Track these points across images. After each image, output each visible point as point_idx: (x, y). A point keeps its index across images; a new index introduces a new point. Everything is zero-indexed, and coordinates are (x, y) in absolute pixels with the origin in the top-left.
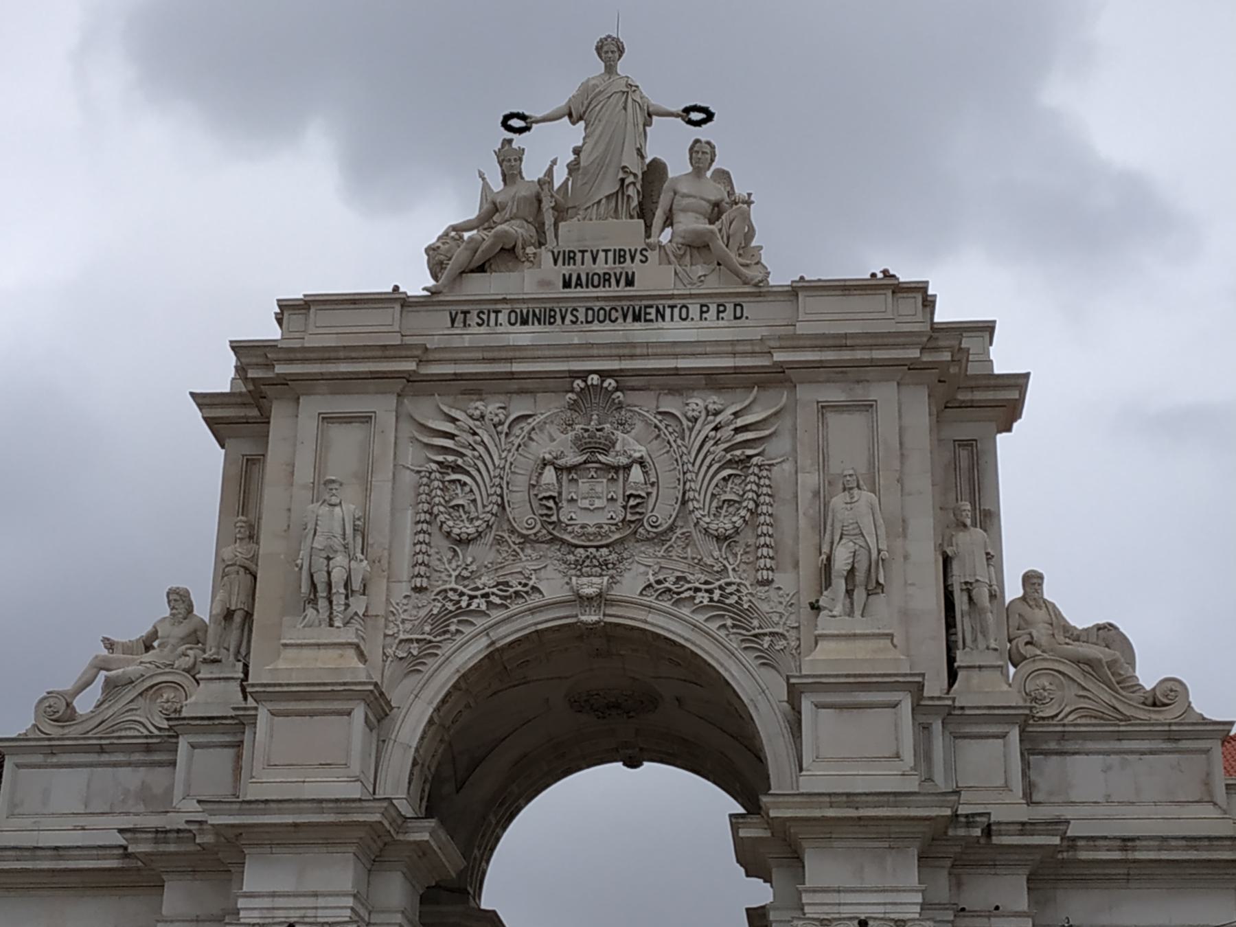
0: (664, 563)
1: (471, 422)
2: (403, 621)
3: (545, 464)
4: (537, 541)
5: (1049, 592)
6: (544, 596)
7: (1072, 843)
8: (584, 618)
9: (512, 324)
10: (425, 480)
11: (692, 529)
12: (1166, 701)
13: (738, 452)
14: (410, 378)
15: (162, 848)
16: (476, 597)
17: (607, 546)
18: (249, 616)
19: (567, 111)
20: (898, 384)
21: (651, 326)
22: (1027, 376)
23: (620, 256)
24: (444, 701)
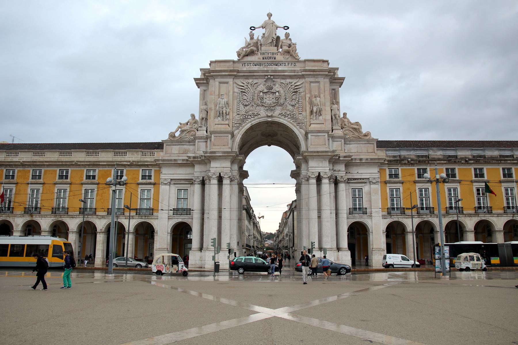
1: (247, 84)
3: (261, 92)
5: (348, 116)
7: (352, 159)
10: (239, 94)
11: (287, 104)
13: (295, 90)
14: (235, 76)
15: (194, 160)
16: (249, 116)
17: (272, 107)
18: (206, 119)
19: (262, 26)
21: (279, 67)
22: (345, 78)
23: (273, 54)
24: (243, 134)
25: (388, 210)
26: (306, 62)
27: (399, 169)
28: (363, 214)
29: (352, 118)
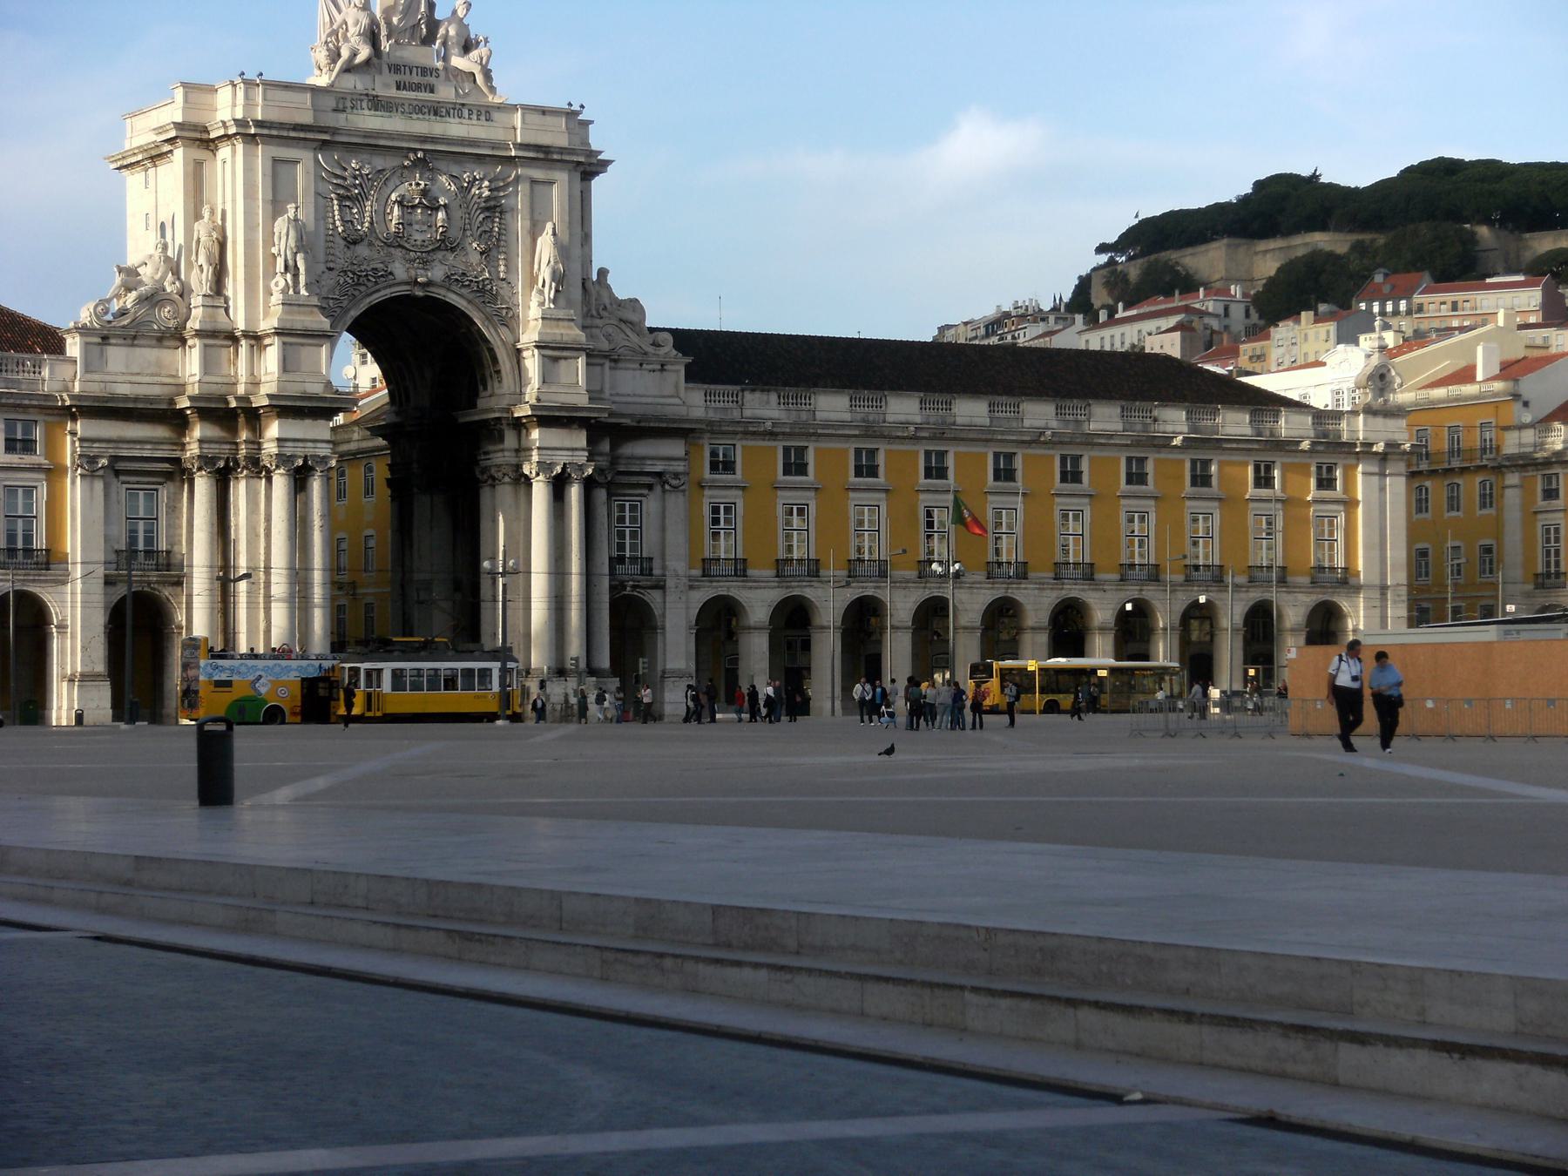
2: (323, 286)
4: (389, 246)
5: (610, 280)
8: (417, 293)
9: (370, 110)
12: (661, 343)
20: (570, 171)
22: (612, 162)
25: (704, 564)
27: (737, 446)
28: (642, 574)
29: (621, 289)
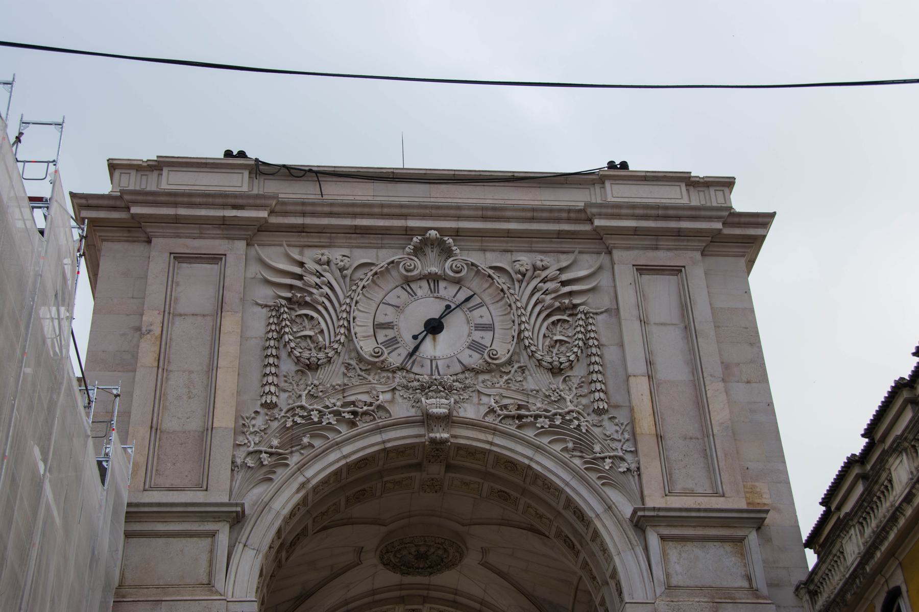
0: (505, 393)
1: (318, 268)
6: (391, 416)
13: (567, 301)
20: (702, 255)
26: (608, 184)
